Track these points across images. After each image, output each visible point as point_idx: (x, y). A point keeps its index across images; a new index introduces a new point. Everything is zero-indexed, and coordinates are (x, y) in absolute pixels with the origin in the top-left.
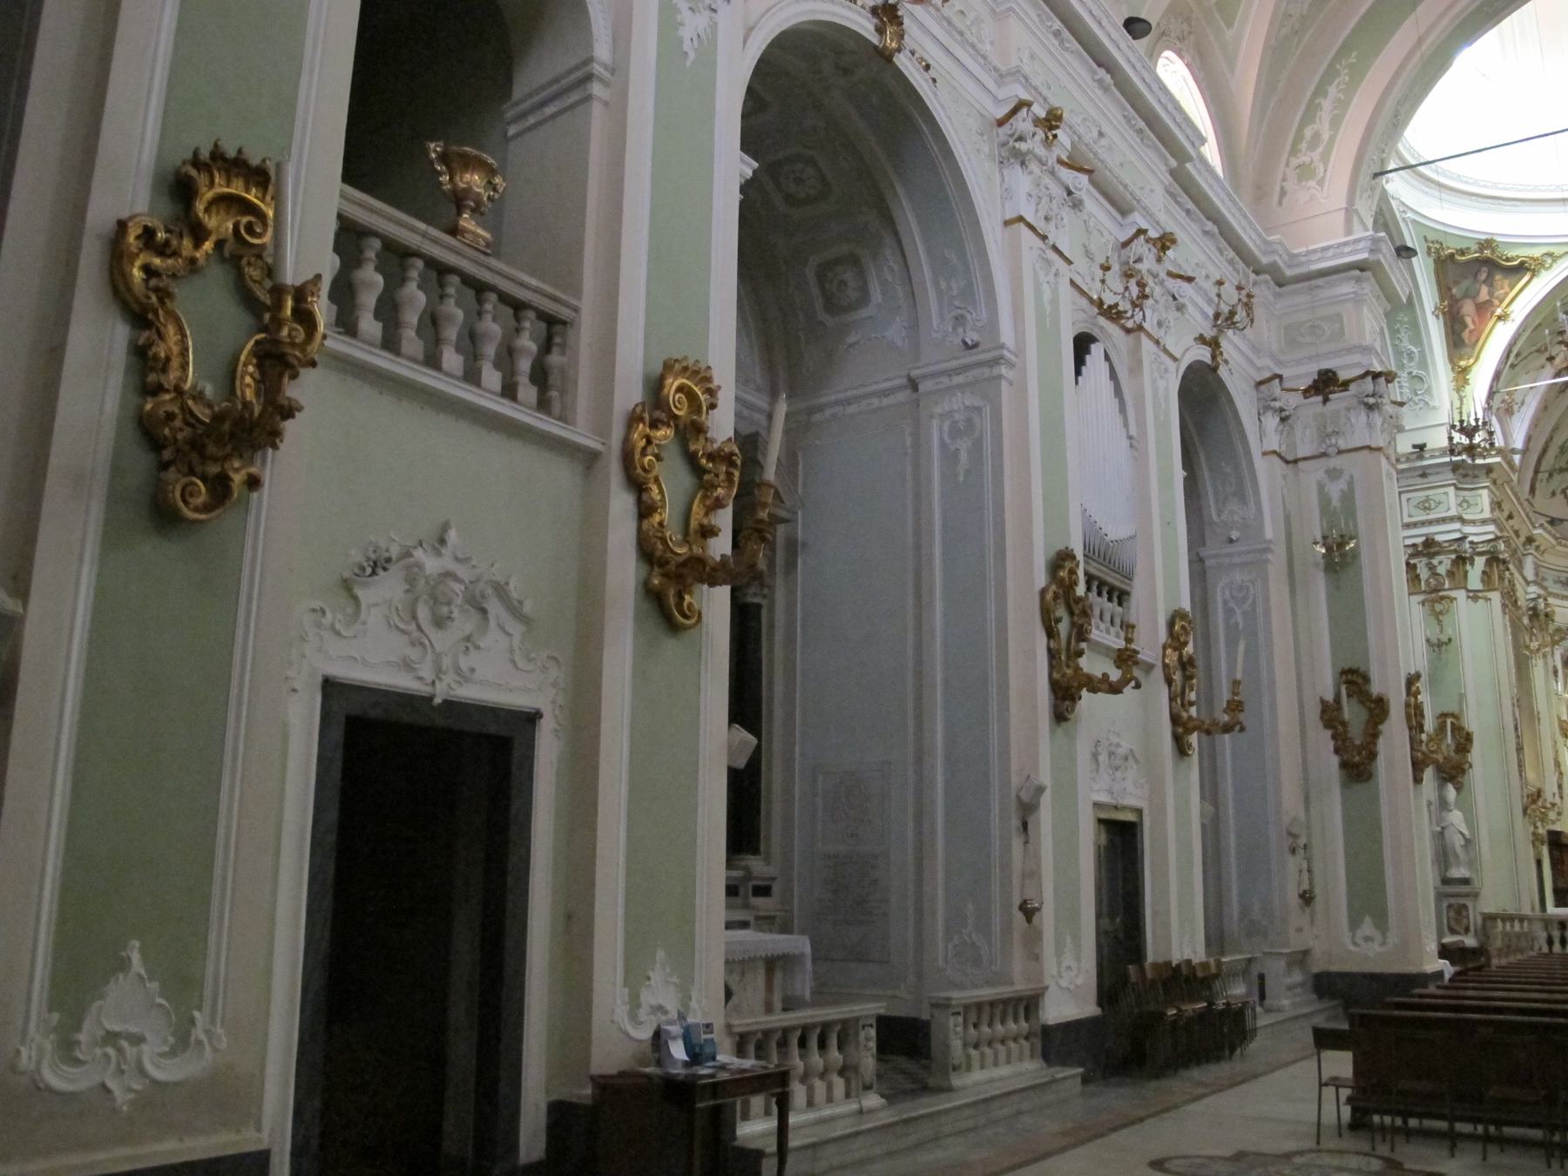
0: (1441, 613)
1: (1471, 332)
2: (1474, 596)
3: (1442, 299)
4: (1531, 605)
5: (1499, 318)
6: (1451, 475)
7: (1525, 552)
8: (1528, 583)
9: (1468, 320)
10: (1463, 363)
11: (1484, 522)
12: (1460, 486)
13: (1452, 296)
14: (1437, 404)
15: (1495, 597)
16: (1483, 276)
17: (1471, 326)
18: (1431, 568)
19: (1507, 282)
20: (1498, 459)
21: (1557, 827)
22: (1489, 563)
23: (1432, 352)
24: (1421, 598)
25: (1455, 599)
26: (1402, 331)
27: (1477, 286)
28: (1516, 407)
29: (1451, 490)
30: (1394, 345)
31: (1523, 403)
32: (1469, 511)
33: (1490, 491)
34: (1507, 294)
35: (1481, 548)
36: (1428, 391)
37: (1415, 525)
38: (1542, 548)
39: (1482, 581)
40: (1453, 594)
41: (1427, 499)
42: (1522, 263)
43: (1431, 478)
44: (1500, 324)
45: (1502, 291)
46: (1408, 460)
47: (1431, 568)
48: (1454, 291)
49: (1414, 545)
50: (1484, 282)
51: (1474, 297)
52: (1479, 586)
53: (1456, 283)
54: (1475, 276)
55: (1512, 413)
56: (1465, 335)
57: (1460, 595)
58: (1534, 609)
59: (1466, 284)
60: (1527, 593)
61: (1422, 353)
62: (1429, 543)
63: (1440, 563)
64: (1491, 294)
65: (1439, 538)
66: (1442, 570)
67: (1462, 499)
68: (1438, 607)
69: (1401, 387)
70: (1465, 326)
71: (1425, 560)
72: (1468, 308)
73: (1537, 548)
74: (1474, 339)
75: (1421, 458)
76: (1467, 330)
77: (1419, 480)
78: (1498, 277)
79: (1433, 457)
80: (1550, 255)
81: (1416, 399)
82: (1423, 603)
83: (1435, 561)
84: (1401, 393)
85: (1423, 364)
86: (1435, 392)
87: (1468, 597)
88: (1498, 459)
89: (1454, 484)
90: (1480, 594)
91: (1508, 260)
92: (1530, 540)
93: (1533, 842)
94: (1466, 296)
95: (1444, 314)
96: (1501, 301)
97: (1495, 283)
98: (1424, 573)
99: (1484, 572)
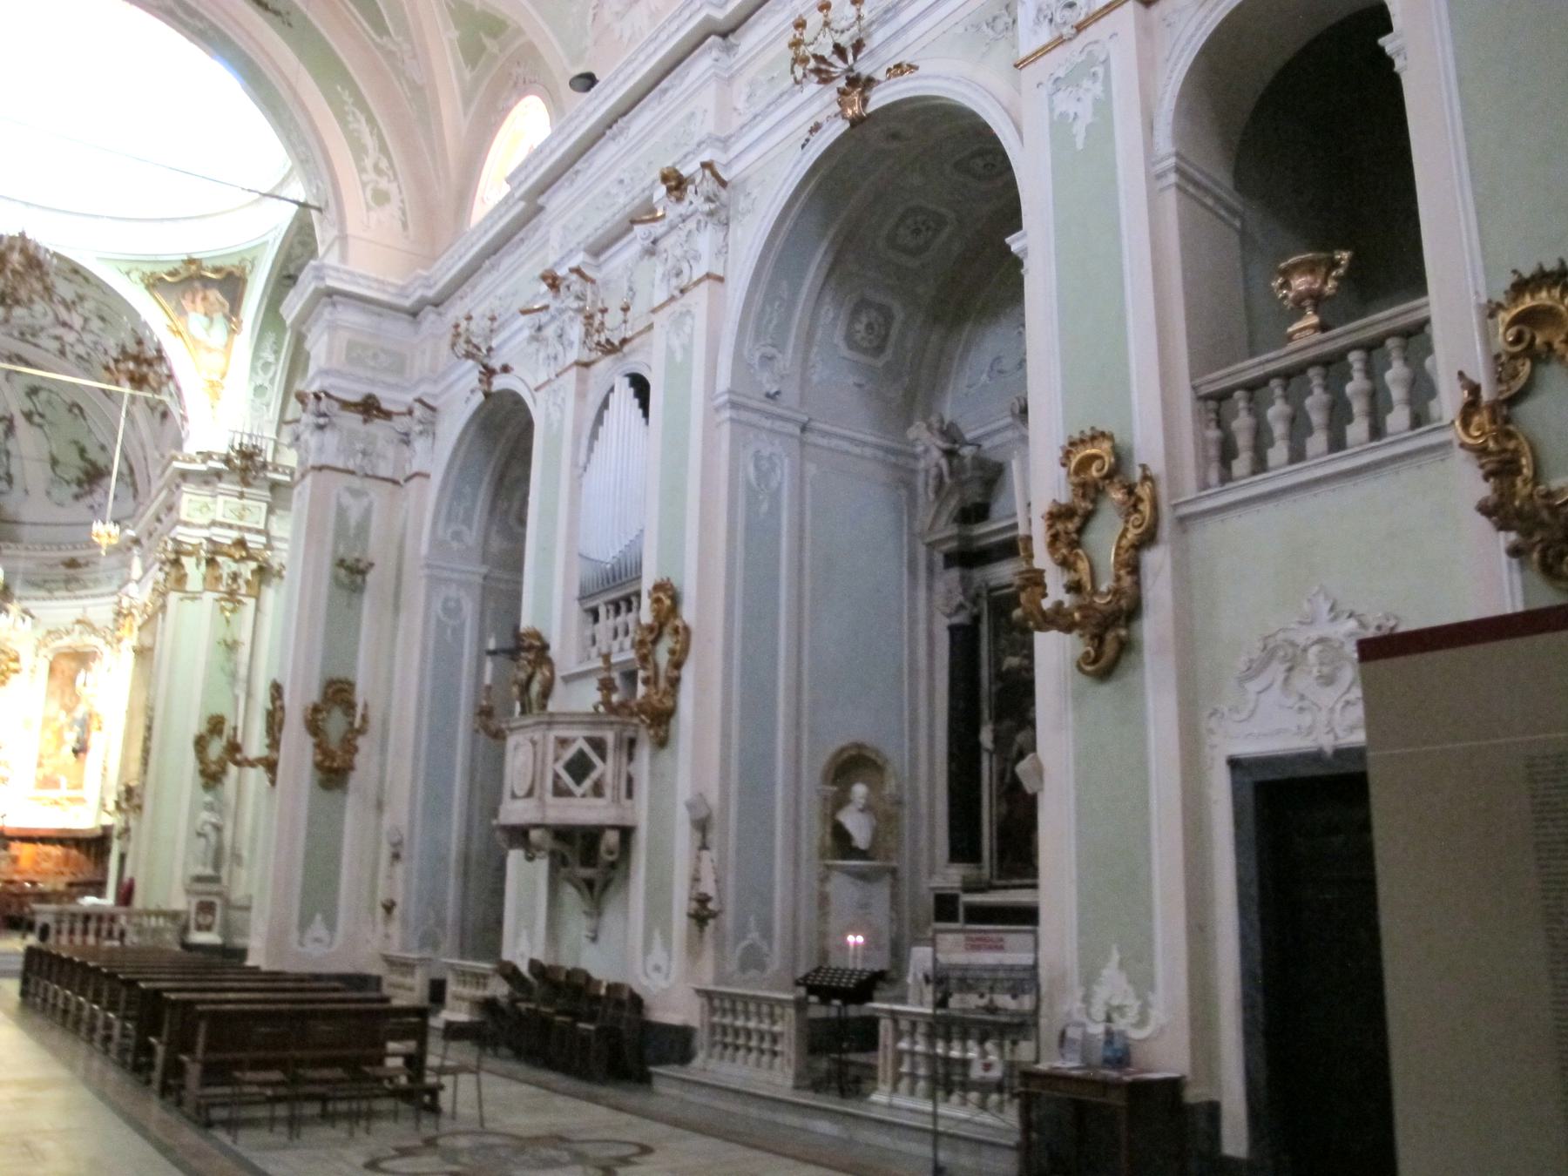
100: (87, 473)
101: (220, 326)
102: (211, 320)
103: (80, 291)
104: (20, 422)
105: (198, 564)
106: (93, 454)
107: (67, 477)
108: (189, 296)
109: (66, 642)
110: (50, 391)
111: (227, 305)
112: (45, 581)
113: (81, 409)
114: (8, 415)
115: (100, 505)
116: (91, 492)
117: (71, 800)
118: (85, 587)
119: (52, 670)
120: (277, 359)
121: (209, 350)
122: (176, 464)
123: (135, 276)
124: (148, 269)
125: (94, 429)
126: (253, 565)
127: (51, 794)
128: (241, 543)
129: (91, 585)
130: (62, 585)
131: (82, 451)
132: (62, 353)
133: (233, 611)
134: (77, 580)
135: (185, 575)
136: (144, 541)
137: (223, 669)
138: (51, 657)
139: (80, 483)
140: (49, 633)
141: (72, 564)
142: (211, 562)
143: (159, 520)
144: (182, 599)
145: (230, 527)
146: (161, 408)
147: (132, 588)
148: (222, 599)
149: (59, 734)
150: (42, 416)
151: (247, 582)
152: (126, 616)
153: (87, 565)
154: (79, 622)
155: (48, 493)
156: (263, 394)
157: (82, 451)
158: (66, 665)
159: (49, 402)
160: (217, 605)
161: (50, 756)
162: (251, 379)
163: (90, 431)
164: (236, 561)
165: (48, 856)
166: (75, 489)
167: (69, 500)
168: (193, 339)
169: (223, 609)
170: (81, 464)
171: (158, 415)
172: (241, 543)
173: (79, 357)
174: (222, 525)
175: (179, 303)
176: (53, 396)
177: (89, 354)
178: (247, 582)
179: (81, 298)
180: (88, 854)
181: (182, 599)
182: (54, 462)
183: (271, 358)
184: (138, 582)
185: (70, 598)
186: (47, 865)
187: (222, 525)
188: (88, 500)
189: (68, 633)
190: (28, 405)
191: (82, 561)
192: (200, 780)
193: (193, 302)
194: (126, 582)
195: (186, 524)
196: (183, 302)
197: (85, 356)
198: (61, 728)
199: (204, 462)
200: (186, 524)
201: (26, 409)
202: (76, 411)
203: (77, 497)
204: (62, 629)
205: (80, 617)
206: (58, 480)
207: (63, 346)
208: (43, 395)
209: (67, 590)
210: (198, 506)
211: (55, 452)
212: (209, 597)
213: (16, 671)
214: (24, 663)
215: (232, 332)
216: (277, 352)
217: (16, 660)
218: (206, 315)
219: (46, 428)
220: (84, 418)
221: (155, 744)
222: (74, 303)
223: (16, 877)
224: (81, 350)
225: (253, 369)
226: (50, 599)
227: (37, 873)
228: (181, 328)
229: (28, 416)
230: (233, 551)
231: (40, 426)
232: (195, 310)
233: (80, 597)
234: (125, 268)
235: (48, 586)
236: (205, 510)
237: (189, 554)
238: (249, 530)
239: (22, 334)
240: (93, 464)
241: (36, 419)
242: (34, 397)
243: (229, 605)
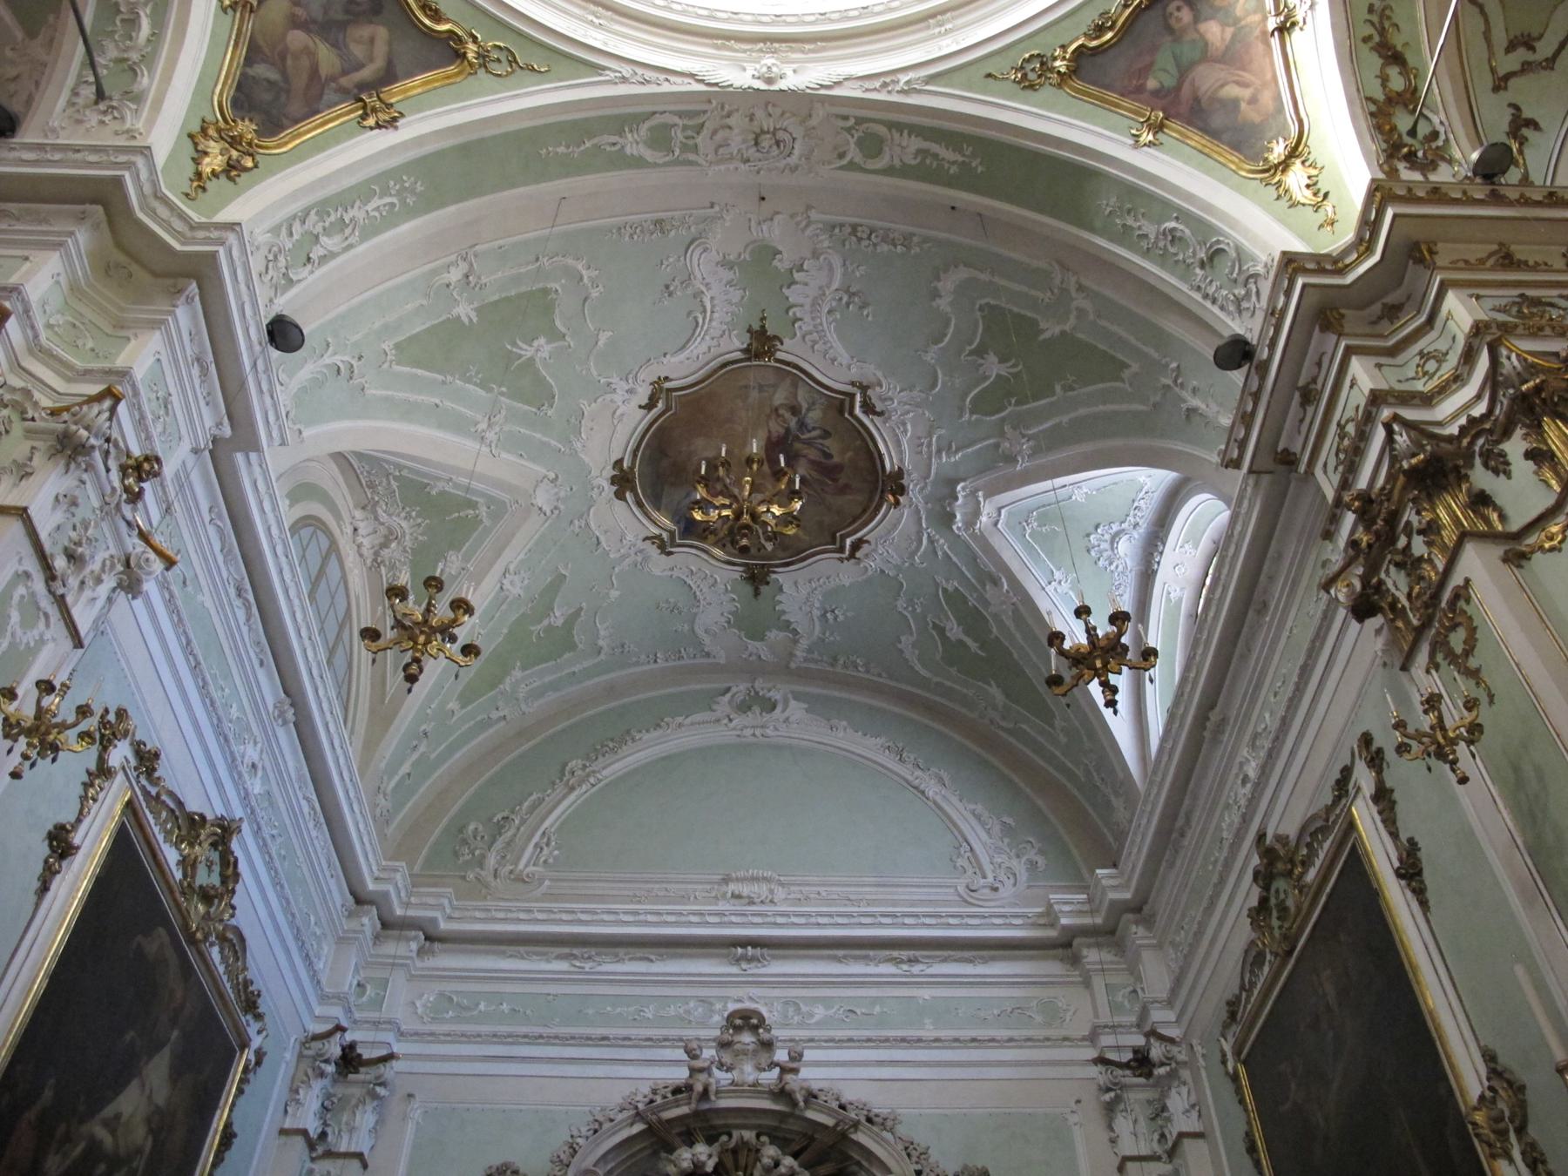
5: (1283, 29)
12: (1391, 342)
13: (1156, 93)
16: (1186, 15)
17: (1246, 93)
20: (1389, 213)
23: (1189, 197)
26: (1130, 222)
27: (1191, 35)
44: (1297, 38)
53: (1145, 71)
59: (1164, 59)
61: (1183, 216)
70: (1235, 102)
75: (1263, 368)
76: (1243, 105)
84: (1222, 308)
85: (1203, 228)
89: (1349, 351)
94: (1184, 71)
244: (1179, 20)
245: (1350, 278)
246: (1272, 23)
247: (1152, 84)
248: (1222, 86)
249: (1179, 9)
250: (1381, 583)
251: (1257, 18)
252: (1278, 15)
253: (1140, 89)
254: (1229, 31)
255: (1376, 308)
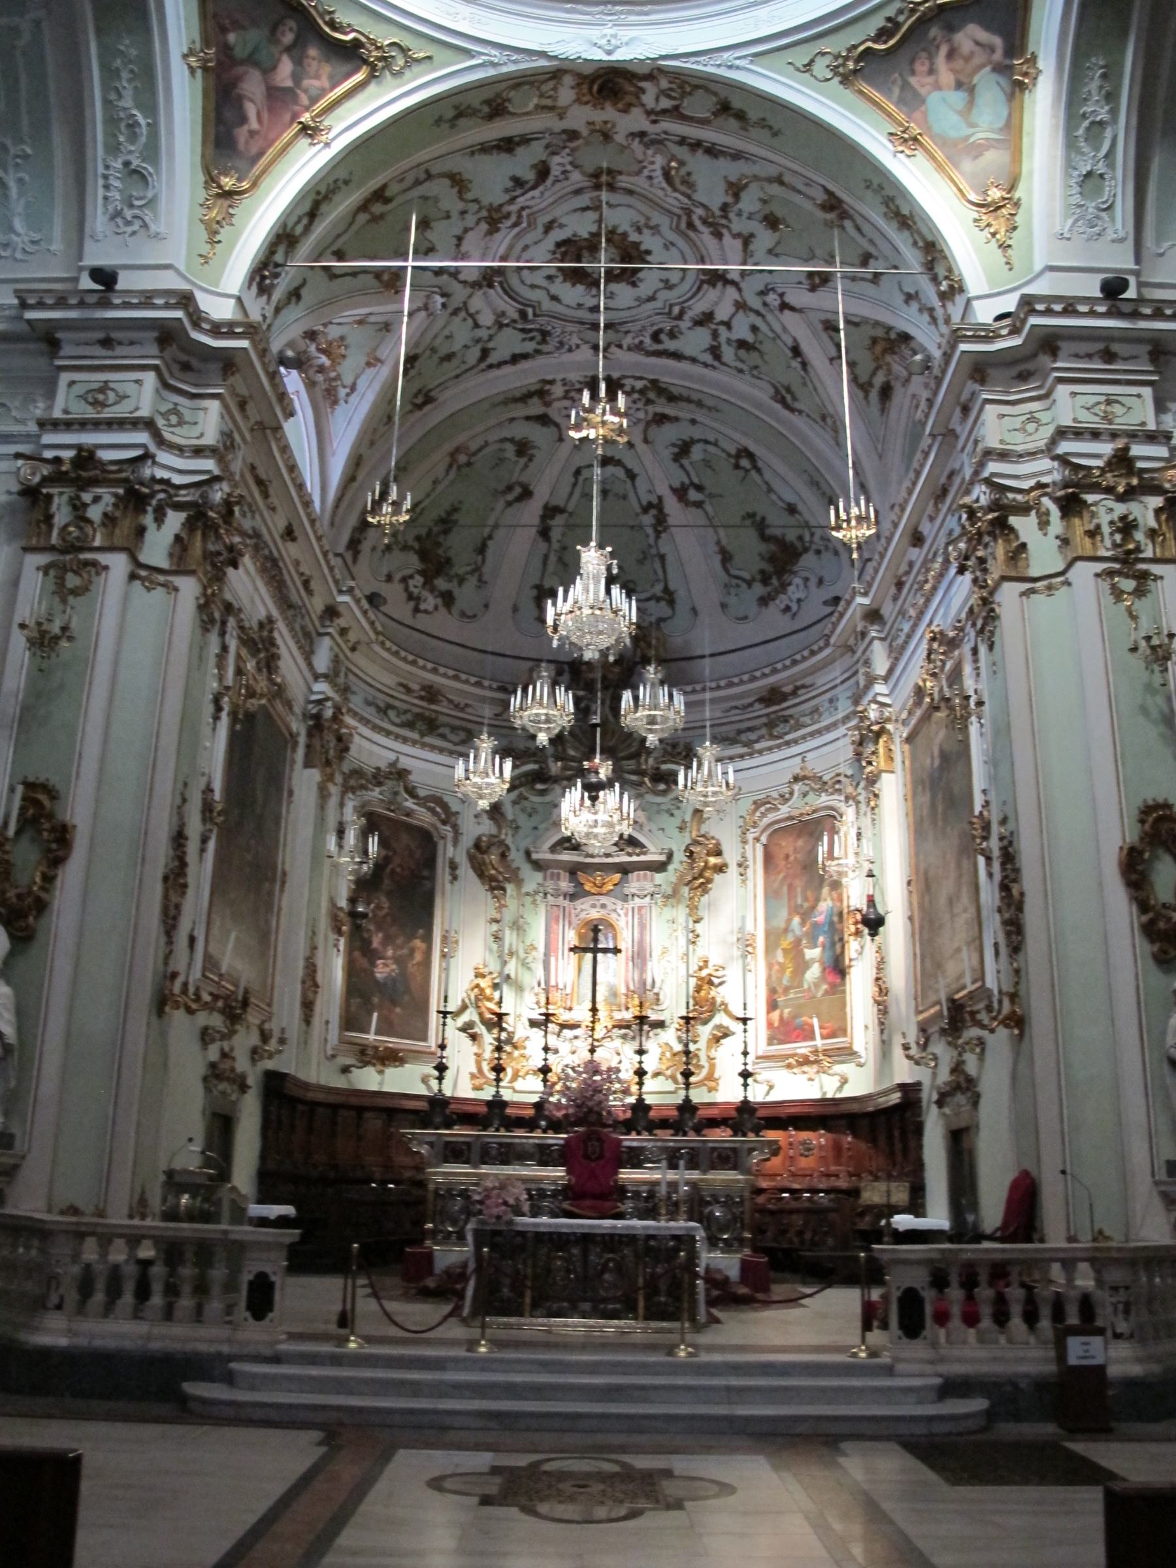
0: (75, 592)
1: (252, 133)
2: (140, 573)
3: (207, 42)
4: (314, 711)
6: (154, 350)
7: (322, 630)
8: (317, 677)
9: (251, 110)
10: (228, 182)
11: (198, 452)
12: (172, 382)
14: (162, 229)
15: (189, 588)
16: (288, 38)
17: (254, 124)
18: (78, 508)
19: (326, 69)
20: (244, 343)
21: (285, 1063)
22: (190, 525)
23: (170, 133)
24: (43, 559)
25: (106, 568)
26: (125, 75)
27: (275, 50)
28: (342, 392)
29: (150, 378)
30: (107, 102)
31: (353, 388)
32: (177, 430)
33: (225, 406)
34: (323, 92)
35: (184, 497)
36: (152, 203)
37: (68, 425)
38: (352, 636)
39: (171, 555)
40: (103, 558)
41: (105, 388)
42: (356, 44)
43: (119, 351)
44: (304, 142)
45: (316, 83)
46: (82, 304)
47: (78, 508)
48: (232, 37)
49: (57, 460)
50: (288, 49)
51: (268, 70)
52: (164, 564)
53: (237, 26)
54: (274, 30)
55: (335, 402)
56: (241, 133)
57: (118, 563)
58: (317, 717)
60: (312, 692)
61: (153, 127)
62: (85, 457)
63: (97, 499)
64: (297, 78)
65: (106, 455)
66: (95, 513)
67: (171, 406)
68: (72, 581)
69: (107, 187)
70: (243, 120)
71: (69, 491)
72: (252, 86)
73: (343, 632)
74: (254, 150)
75: (105, 304)
76: (246, 128)
77: (99, 351)
78: (313, 52)
79: (127, 306)
80: (404, 50)
81: (128, 214)
82: (46, 569)
83: (87, 497)
84: (106, 198)
85: (152, 152)
86: (163, 205)
87: (133, 577)
88: (244, 343)
89: (155, 368)
90: (161, 578)
91: (332, 24)
92: (331, 612)
93: (205, 1079)
94: (252, 60)
95: (205, 69)
96: (314, 101)
97: (306, 61)
98: (61, 514)
99: (178, 538)
100: (772, 559)
101: (990, 88)
102: (971, 90)
103: (734, 170)
104: (672, 506)
105: (1044, 524)
106: (778, 522)
107: (746, 575)
108: (921, 67)
109: (784, 810)
110: (706, 442)
111: (997, 41)
112: (739, 732)
113: (751, 456)
114: (655, 501)
115: (799, 601)
116: (784, 586)
117: (827, 1053)
118: (799, 726)
119: (768, 858)
120: (1114, 112)
121: (976, 150)
122: (963, 347)
123: (821, 68)
124: (838, 44)
125: (777, 485)
126: (1157, 501)
127: (803, 1048)
128: (1122, 461)
129: (807, 720)
130: (764, 731)
131: (761, 526)
132: (715, 351)
133: (1139, 592)
134: (786, 720)
135: (1023, 546)
136: (888, 610)
137: (1144, 710)
138: (764, 839)
139: (765, 579)
140: (757, 804)
141: (773, 696)
142: (1071, 506)
143: (917, 539)
144: (1026, 594)
145: (1095, 435)
146: (879, 380)
147: (879, 688)
148: (1110, 573)
149: (796, 952)
150: (699, 488)
151: (1152, 534)
152: (878, 735)
153: (794, 693)
154: (796, 779)
155: (724, 606)
156: (1099, 191)
157: (761, 526)
158: (789, 846)
159: (707, 463)
160: (1105, 585)
161: (786, 990)
162: (1069, 165)
163: (770, 490)
164: (1122, 498)
165: (808, 1148)
166: (759, 589)
167: (753, 608)
168: (944, 142)
169: (1117, 593)
170: (763, 548)
171: (874, 395)
172: (1122, 461)
173: (742, 344)
174: (1078, 433)
175: (905, 86)
176: (711, 449)
177: (754, 329)
178: (1152, 534)
179: (736, 189)
180: (873, 1140)
181: (1026, 594)
182: (726, 557)
183: (1103, 114)
184: (886, 679)
185: (779, 747)
186: (804, 1163)
187: (1078, 433)
188: (782, 601)
189: (784, 799)
190: (679, 477)
191: (788, 689)
192: (1145, 948)
193: (931, 71)
194: (871, 680)
195: (1004, 456)
196: (913, 80)
197: (750, 338)
198: (797, 942)
199: (1015, 331)
200: (1004, 456)
201: (677, 484)
202: (745, 463)
203: (764, 601)
204: (775, 795)
205: (797, 771)
206: (733, 582)
207: (715, 335)
208: (697, 452)
209: (773, 737)
210: (1017, 422)
211: (724, 542)
212: (1084, 573)
213: (720, 869)
214: (731, 856)
215: (1018, 88)
216: (1111, 97)
217: (719, 853)
218: (959, 85)
219: (708, 507)
220: (759, 470)
221: (1030, 883)
222: (725, 208)
223: (764, 1184)
224: (741, 330)
225: (1071, 144)
226: (751, 754)
227: (793, 1175)
228: (915, 130)
229: (680, 493)
230: (1109, 479)
231: (699, 505)
232: (938, 87)
233: (795, 742)
234: (801, 57)
235: (743, 737)
236: (1031, 427)
237: (1024, 510)
238: (1133, 435)
239: (656, 337)
240: (780, 542)
241: (693, 495)
242: (685, 462)
243: (1128, 585)
244: (283, 34)
245: (196, 335)
246: (306, 117)
247: (232, 37)
248: (252, 100)
249: (291, 29)
250: (49, 497)
251: (305, 101)
252: (313, 119)
253: (224, 30)
254: (289, 83)
255: (184, 358)
